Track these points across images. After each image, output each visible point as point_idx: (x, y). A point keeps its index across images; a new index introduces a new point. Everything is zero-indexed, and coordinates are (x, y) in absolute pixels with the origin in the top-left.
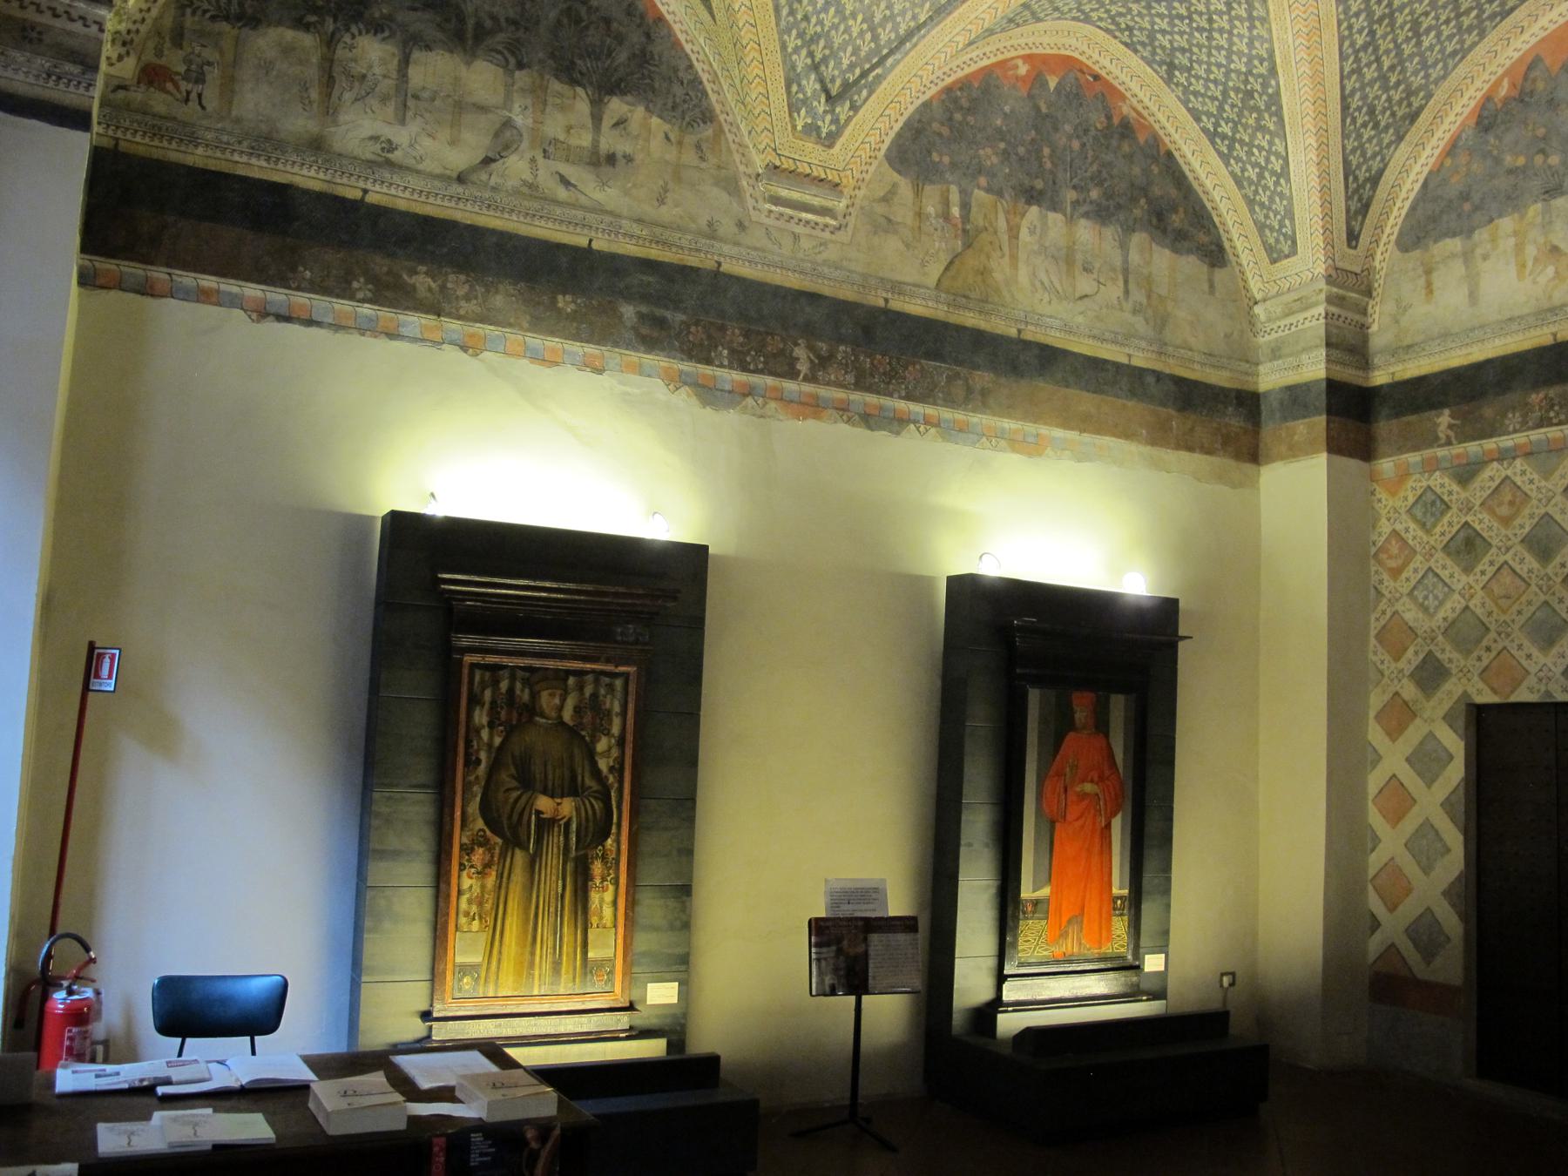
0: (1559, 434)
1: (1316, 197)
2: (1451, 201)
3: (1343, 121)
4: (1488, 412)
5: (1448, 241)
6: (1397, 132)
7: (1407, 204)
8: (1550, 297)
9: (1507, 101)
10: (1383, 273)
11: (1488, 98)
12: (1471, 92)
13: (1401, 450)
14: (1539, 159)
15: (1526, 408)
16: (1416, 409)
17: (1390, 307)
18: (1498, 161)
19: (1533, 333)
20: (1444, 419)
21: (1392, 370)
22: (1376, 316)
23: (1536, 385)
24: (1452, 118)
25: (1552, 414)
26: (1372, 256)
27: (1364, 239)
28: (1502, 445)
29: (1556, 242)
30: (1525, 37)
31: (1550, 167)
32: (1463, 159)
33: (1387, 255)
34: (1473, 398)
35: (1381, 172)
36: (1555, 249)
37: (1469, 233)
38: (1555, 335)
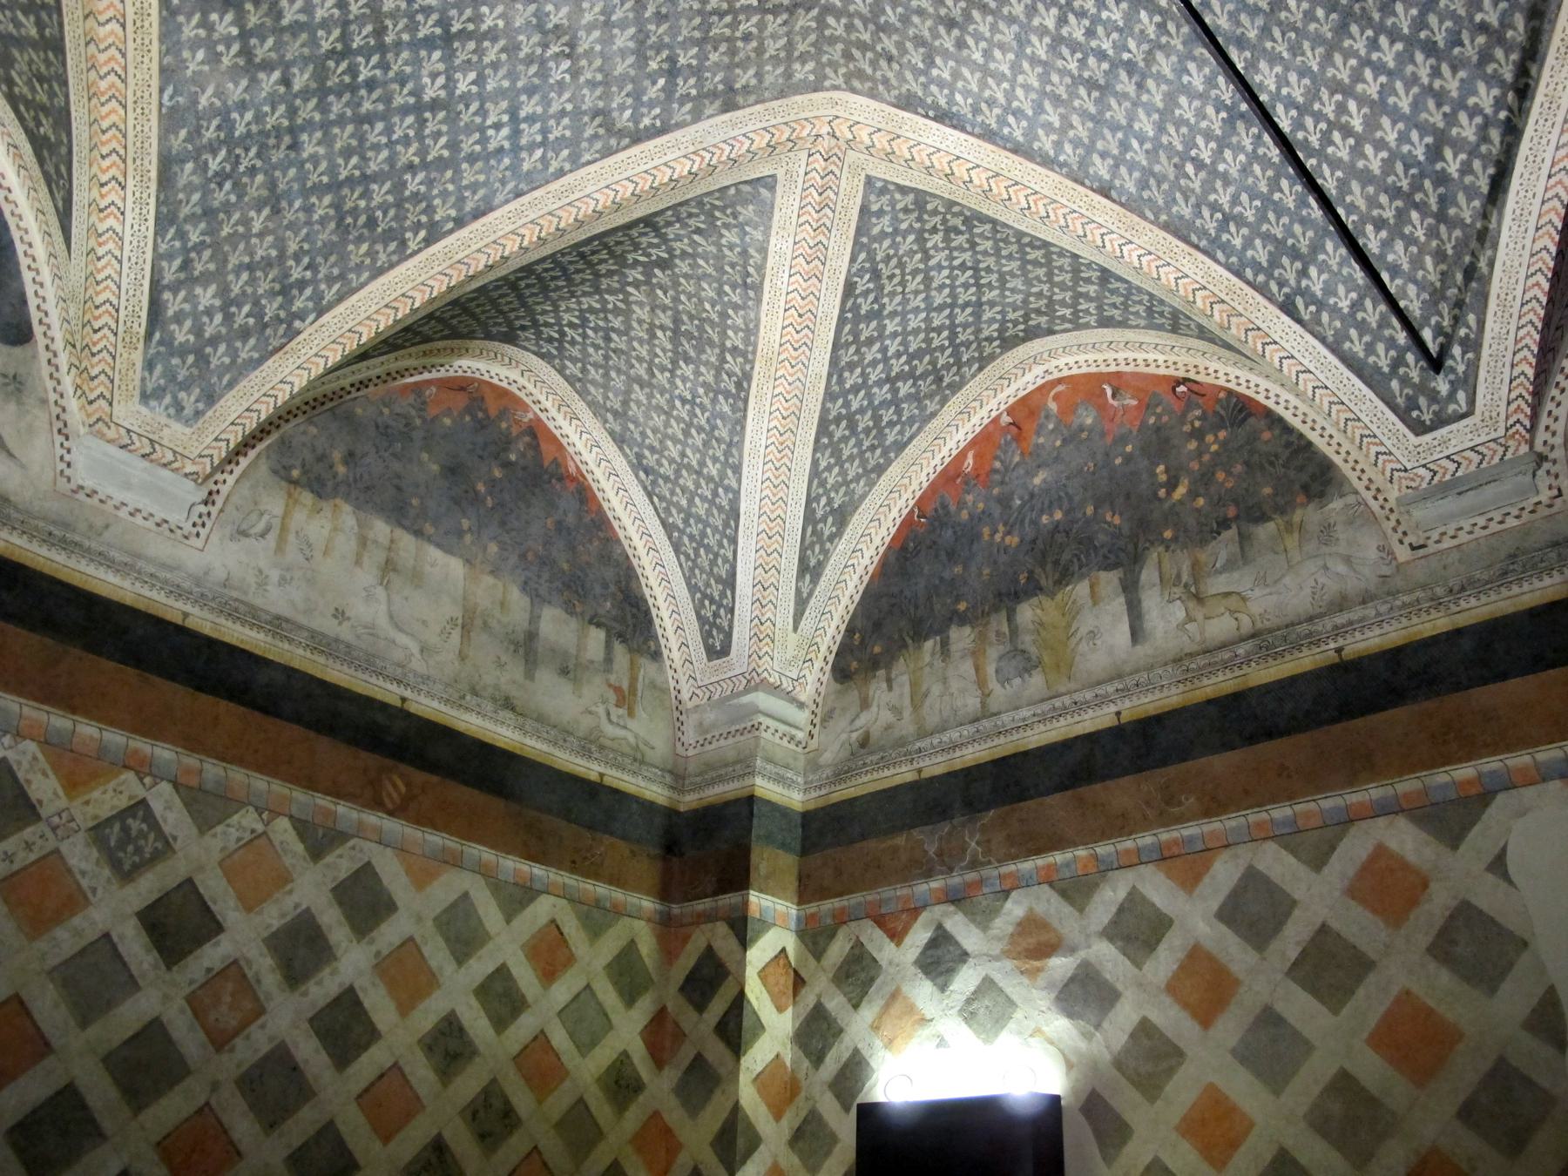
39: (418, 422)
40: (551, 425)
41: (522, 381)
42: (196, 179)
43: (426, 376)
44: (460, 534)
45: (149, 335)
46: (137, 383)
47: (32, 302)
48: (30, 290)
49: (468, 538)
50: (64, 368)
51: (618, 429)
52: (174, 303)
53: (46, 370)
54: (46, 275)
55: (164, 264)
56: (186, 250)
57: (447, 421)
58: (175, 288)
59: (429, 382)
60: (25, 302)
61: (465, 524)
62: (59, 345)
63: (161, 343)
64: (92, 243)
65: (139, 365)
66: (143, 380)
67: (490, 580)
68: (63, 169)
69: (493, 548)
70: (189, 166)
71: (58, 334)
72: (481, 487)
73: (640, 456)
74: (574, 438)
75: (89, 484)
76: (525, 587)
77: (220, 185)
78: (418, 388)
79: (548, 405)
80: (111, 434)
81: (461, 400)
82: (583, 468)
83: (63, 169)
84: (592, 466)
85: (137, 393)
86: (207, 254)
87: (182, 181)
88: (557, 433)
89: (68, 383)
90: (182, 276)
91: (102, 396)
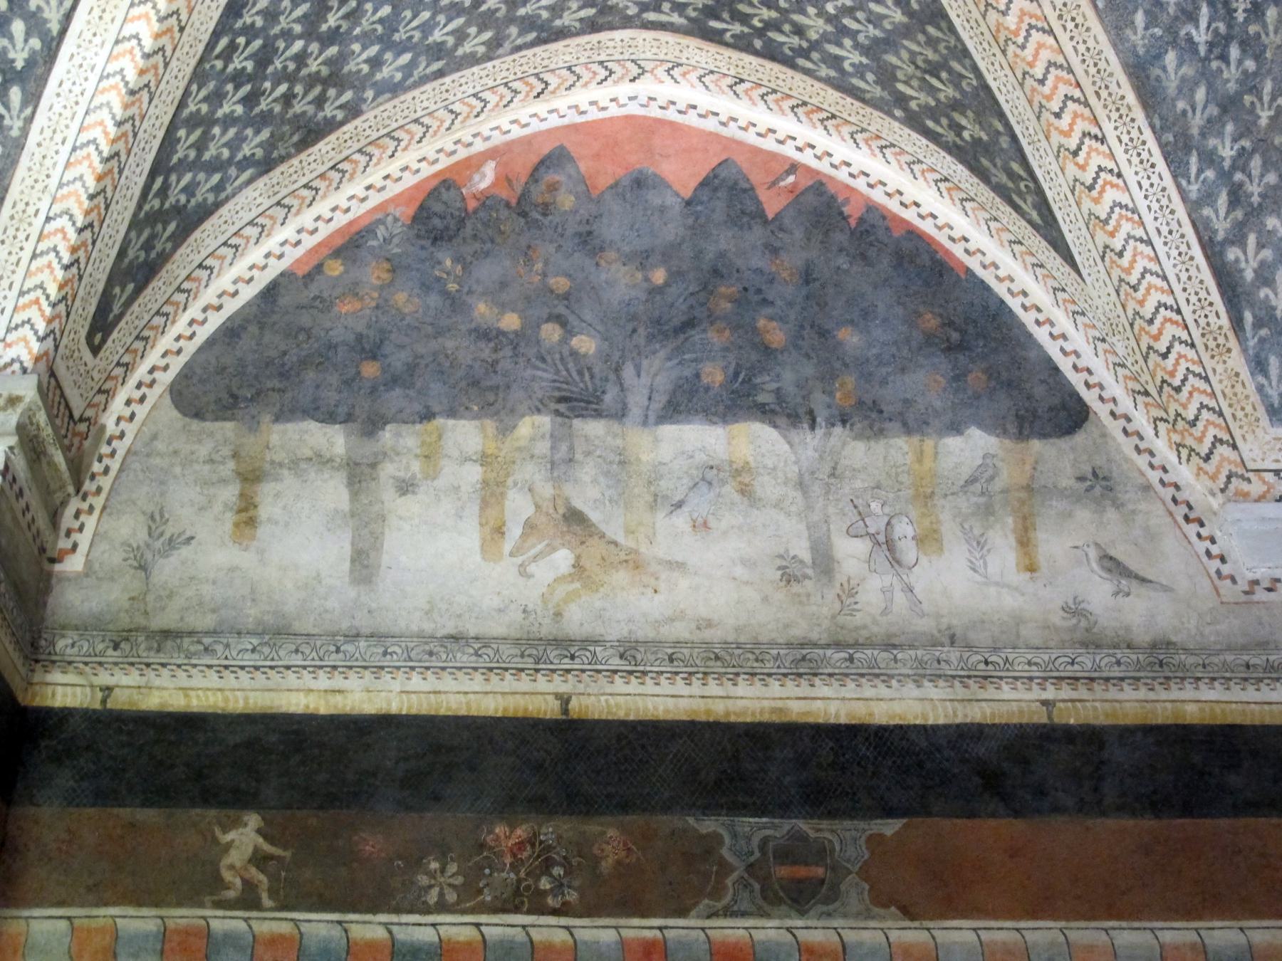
0: (560, 937)
1: (88, 170)
2: (332, 347)
3: (216, 35)
4: (371, 844)
5: (312, 425)
6: (269, 145)
7: (215, 321)
8: (558, 614)
9: (486, 201)
10: (121, 447)
11: (446, 184)
12: (409, 157)
13: (99, 894)
14: (551, 333)
15: (479, 857)
16: (161, 793)
17: (129, 527)
18: (456, 304)
19: (509, 683)
20: (244, 838)
21: (104, 678)
22: (84, 540)
23: (509, 807)
24: (357, 188)
25: (545, 884)
26: (108, 394)
27: (120, 337)
28: (401, 934)
29: (578, 504)
30: (541, 107)
31: (574, 354)
32: (374, 274)
33: (142, 411)
34: (330, 800)
35: (206, 212)
36: (574, 518)
37: (373, 425)
38: (565, 700)
42: (1187, 70)
45: (1237, 324)
46: (1255, 398)
47: (1065, 365)
48: (1053, 349)
50: (1148, 431)
52: (1247, 259)
53: (1127, 445)
54: (1064, 322)
55: (1207, 211)
56: (1225, 176)
58: (1238, 238)
60: (1056, 369)
62: (1126, 404)
63: (1258, 324)
64: (1101, 238)
65: (1245, 374)
66: (1260, 389)
68: (1015, 167)
70: (1171, 58)
71: (1115, 389)
75: (1262, 572)
77: (1224, 58)
80: (1256, 488)
83: (1015, 167)
85: (1261, 412)
86: (1256, 163)
87: (1172, 85)
89: (1162, 447)
90: (1239, 214)
91: (1217, 441)
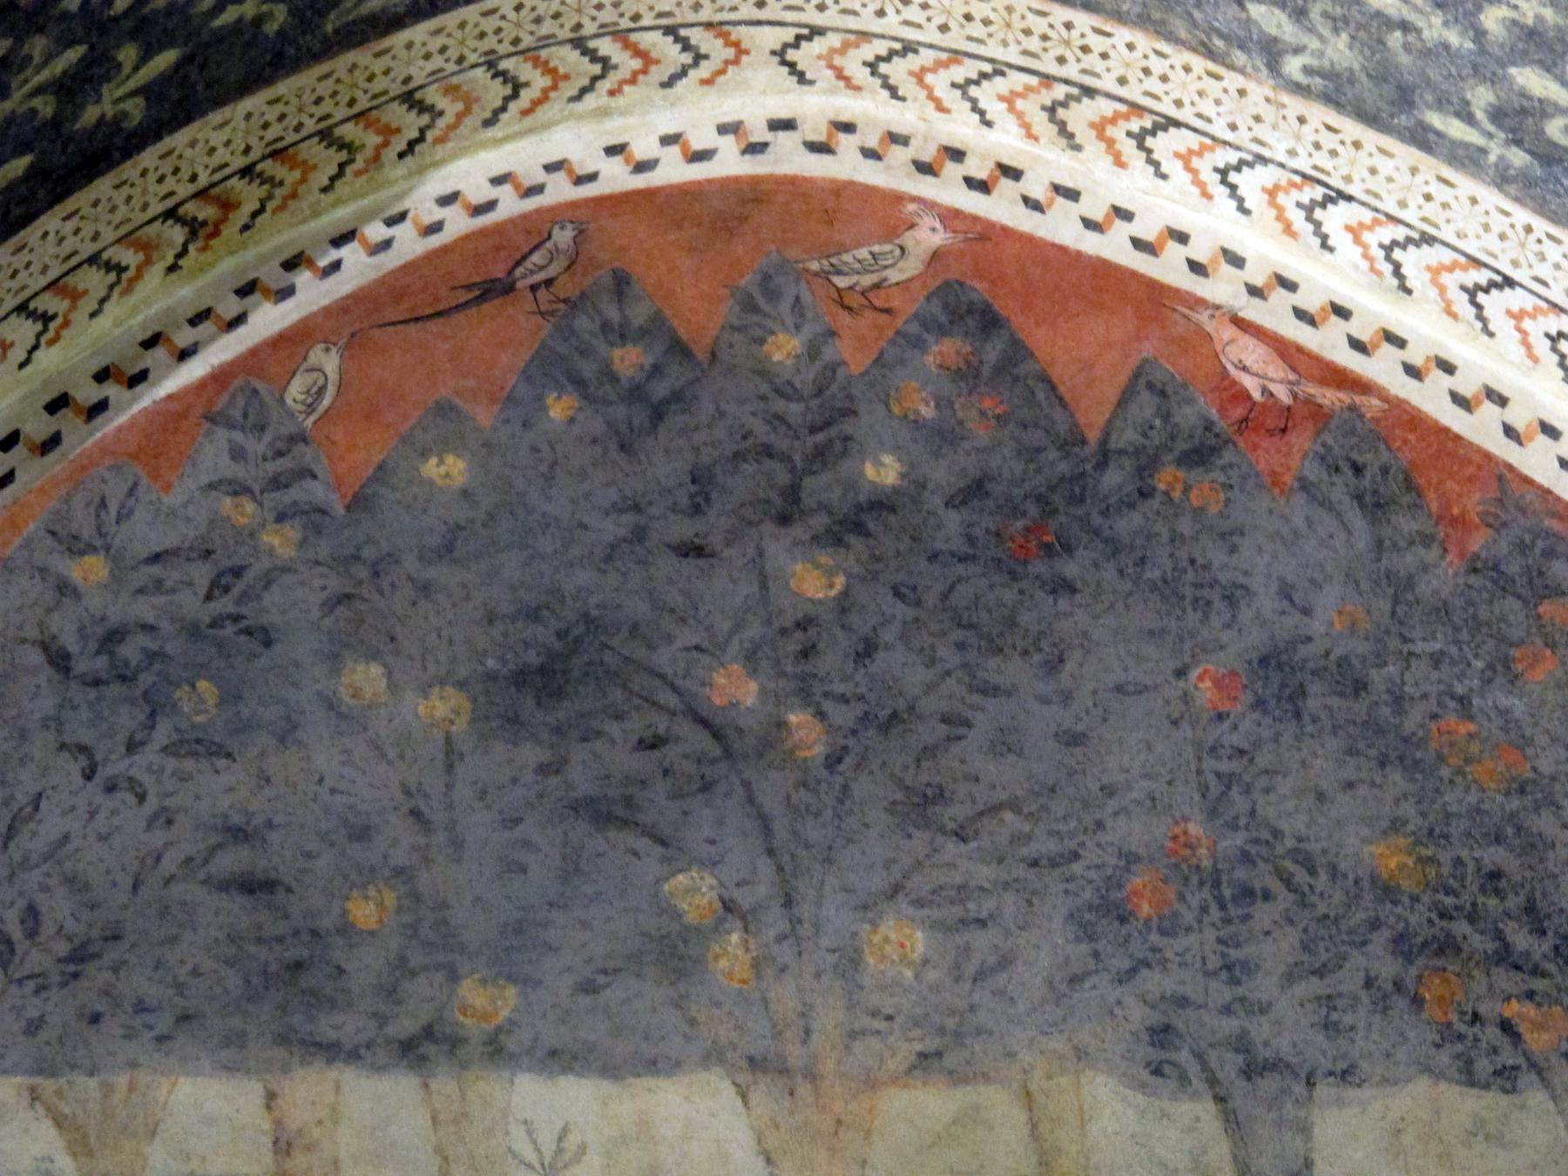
39: (280, 542)
40: (1061, 227)
41: (816, 106)
43: (268, 319)
44: (675, 953)
49: (731, 953)
51: (1340, 51)
57: (448, 470)
59: (292, 342)
61: (693, 892)
67: (933, 1103)
69: (901, 943)
72: (736, 689)
73: (1518, 118)
74: (1214, 224)
76: (1162, 1055)
78: (238, 396)
79: (1006, 141)
81: (506, 339)
82: (1329, 343)
84: (1375, 306)
88: (1114, 247)
